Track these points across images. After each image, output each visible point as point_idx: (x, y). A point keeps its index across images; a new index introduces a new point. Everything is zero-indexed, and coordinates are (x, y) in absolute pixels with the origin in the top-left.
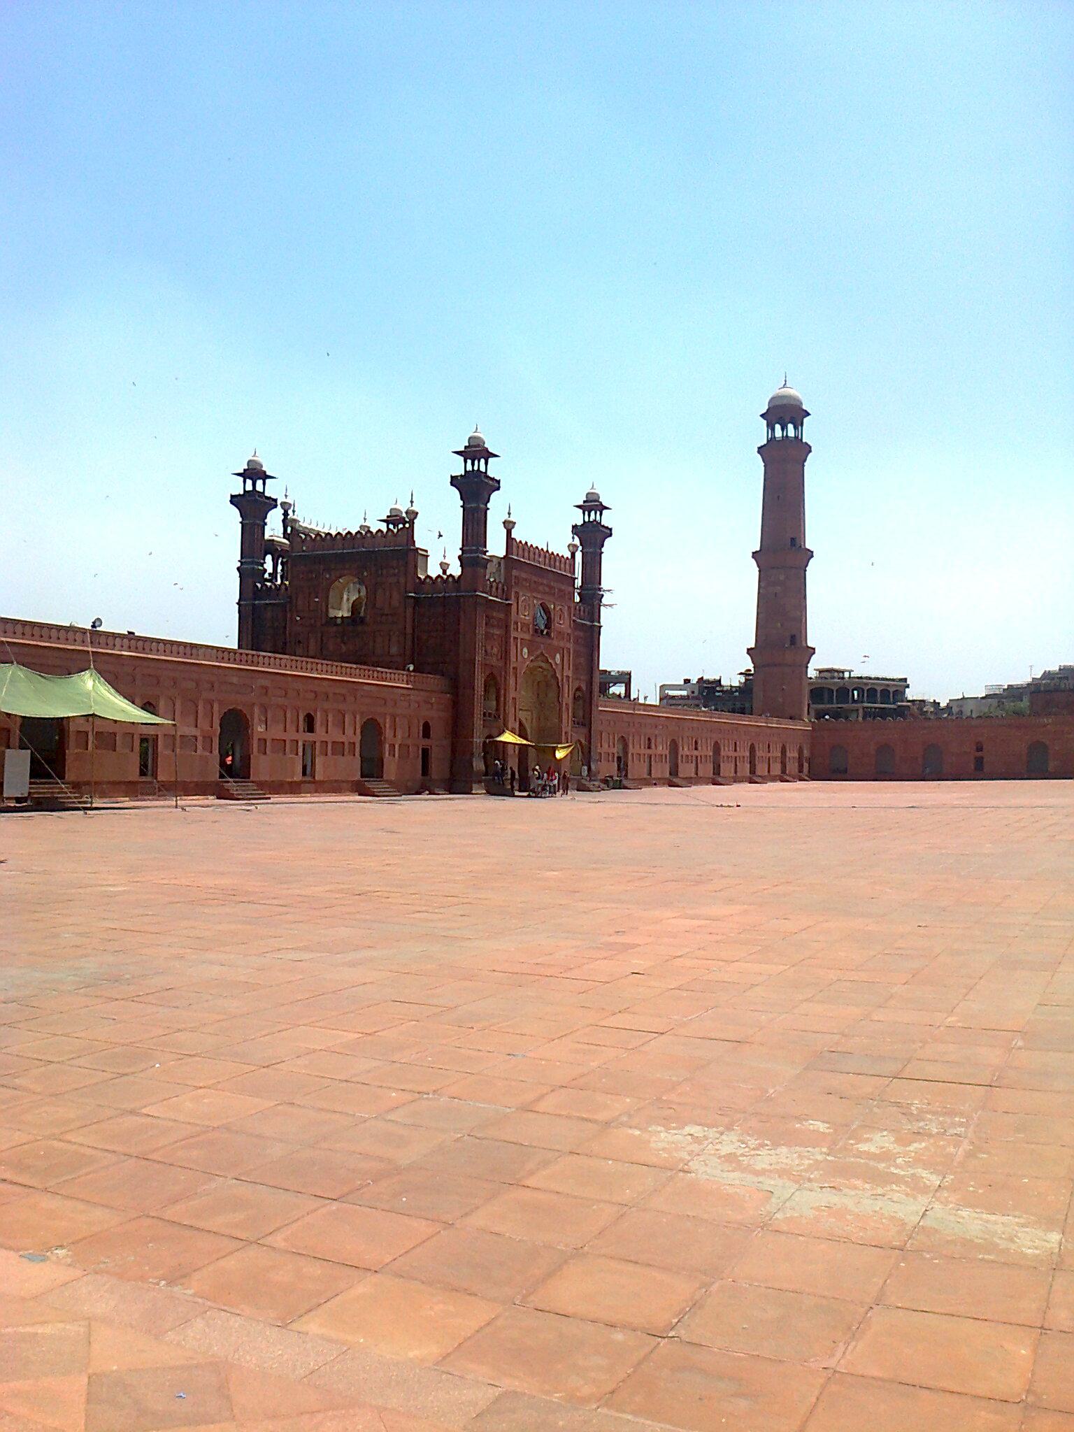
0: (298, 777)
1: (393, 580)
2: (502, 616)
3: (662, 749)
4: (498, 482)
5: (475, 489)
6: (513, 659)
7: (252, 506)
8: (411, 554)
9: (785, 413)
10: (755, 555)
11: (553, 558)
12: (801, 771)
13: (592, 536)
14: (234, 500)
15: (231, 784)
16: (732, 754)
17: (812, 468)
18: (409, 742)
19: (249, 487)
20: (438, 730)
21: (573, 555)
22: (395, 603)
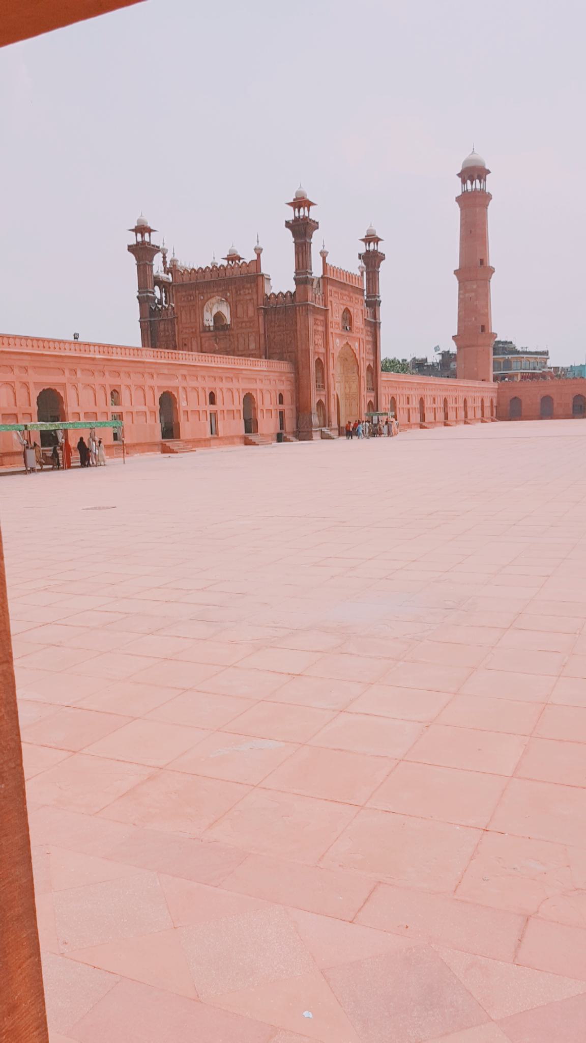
1: (248, 297)
3: (415, 404)
5: (302, 230)
7: (143, 252)
8: (260, 278)
9: (473, 172)
10: (456, 272)
11: (350, 276)
12: (492, 415)
13: (372, 260)
14: (131, 249)
15: (170, 443)
16: (454, 405)
17: (493, 210)
18: (271, 408)
19: (139, 239)
20: (287, 398)
21: (362, 273)
22: (251, 313)
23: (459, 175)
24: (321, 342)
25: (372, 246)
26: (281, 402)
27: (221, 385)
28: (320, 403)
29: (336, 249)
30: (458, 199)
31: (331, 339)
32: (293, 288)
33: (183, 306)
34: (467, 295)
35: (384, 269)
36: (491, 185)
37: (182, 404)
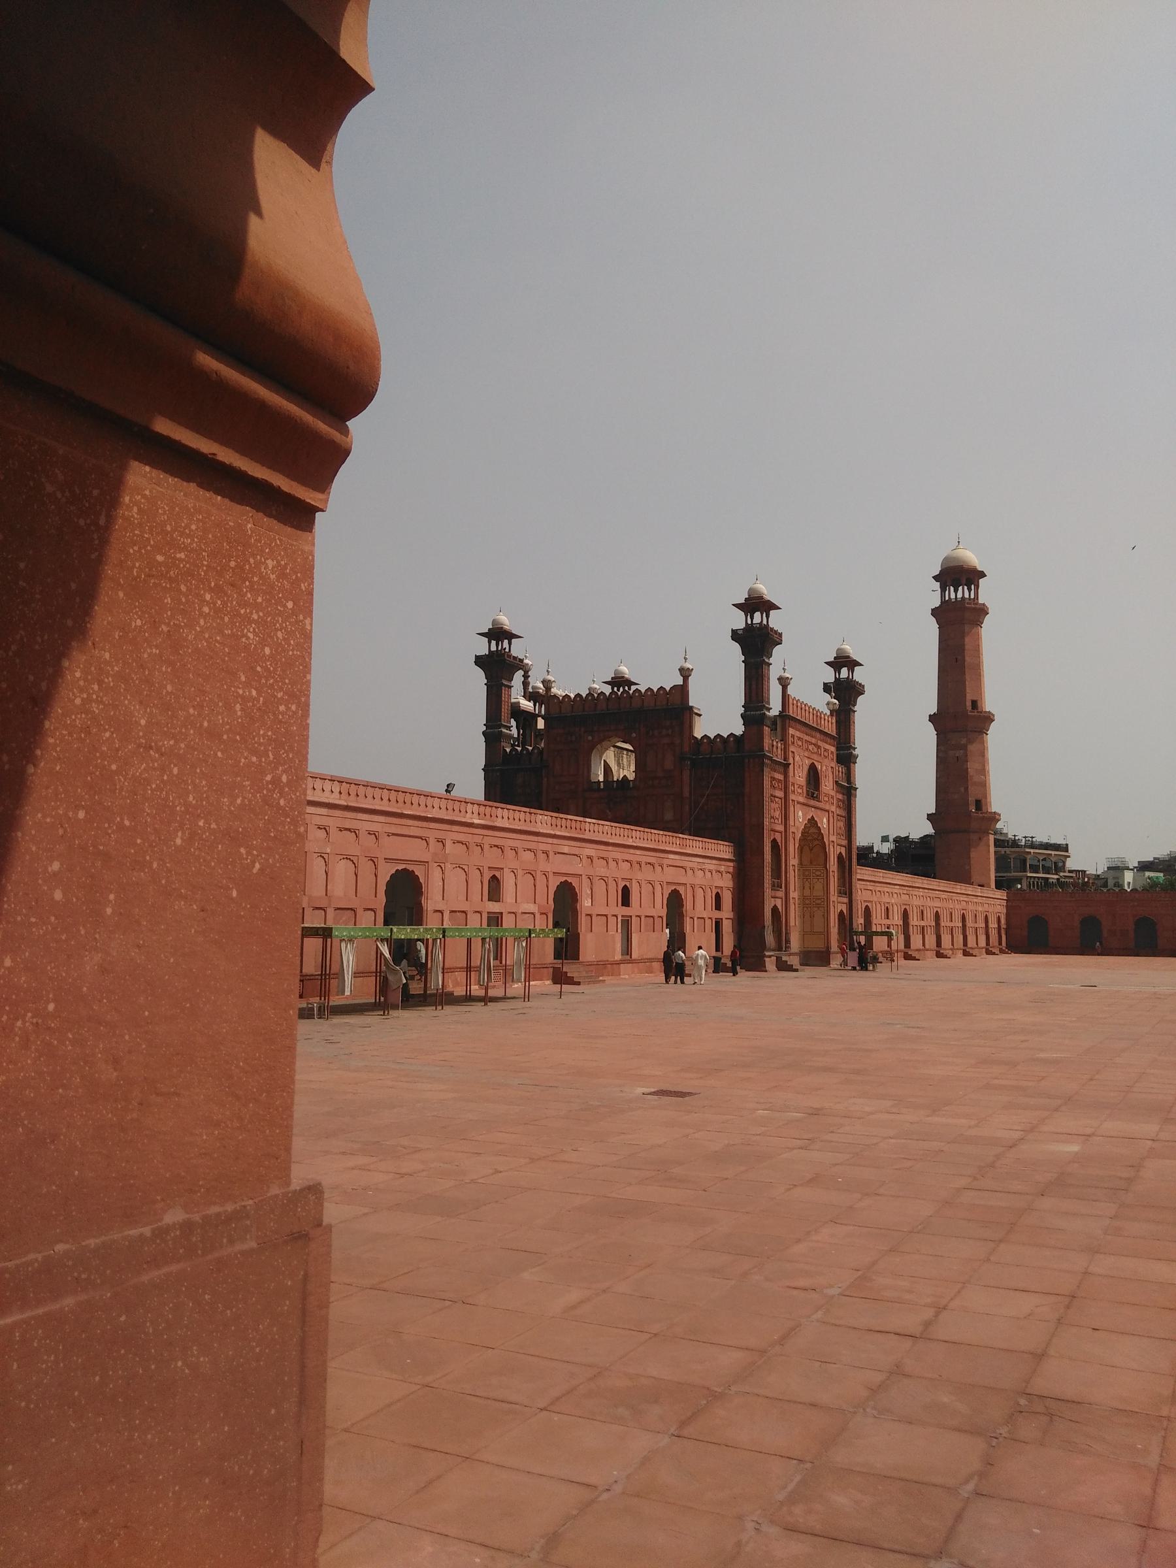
0: (618, 957)
2: (781, 777)
3: (897, 919)
4: (780, 635)
5: (756, 643)
6: (792, 823)
7: (498, 666)
10: (932, 718)
11: (818, 715)
12: (1000, 943)
14: (480, 661)
16: (949, 924)
17: (989, 631)
19: (493, 648)
22: (669, 764)
23: (936, 578)
24: (777, 814)
25: (844, 673)
26: (718, 907)
27: (639, 876)
28: (775, 910)
29: (801, 676)
30: (935, 612)
31: (792, 808)
32: (738, 729)
33: (547, 751)
34: (951, 753)
35: (862, 708)
36: (986, 593)
37: (585, 903)
